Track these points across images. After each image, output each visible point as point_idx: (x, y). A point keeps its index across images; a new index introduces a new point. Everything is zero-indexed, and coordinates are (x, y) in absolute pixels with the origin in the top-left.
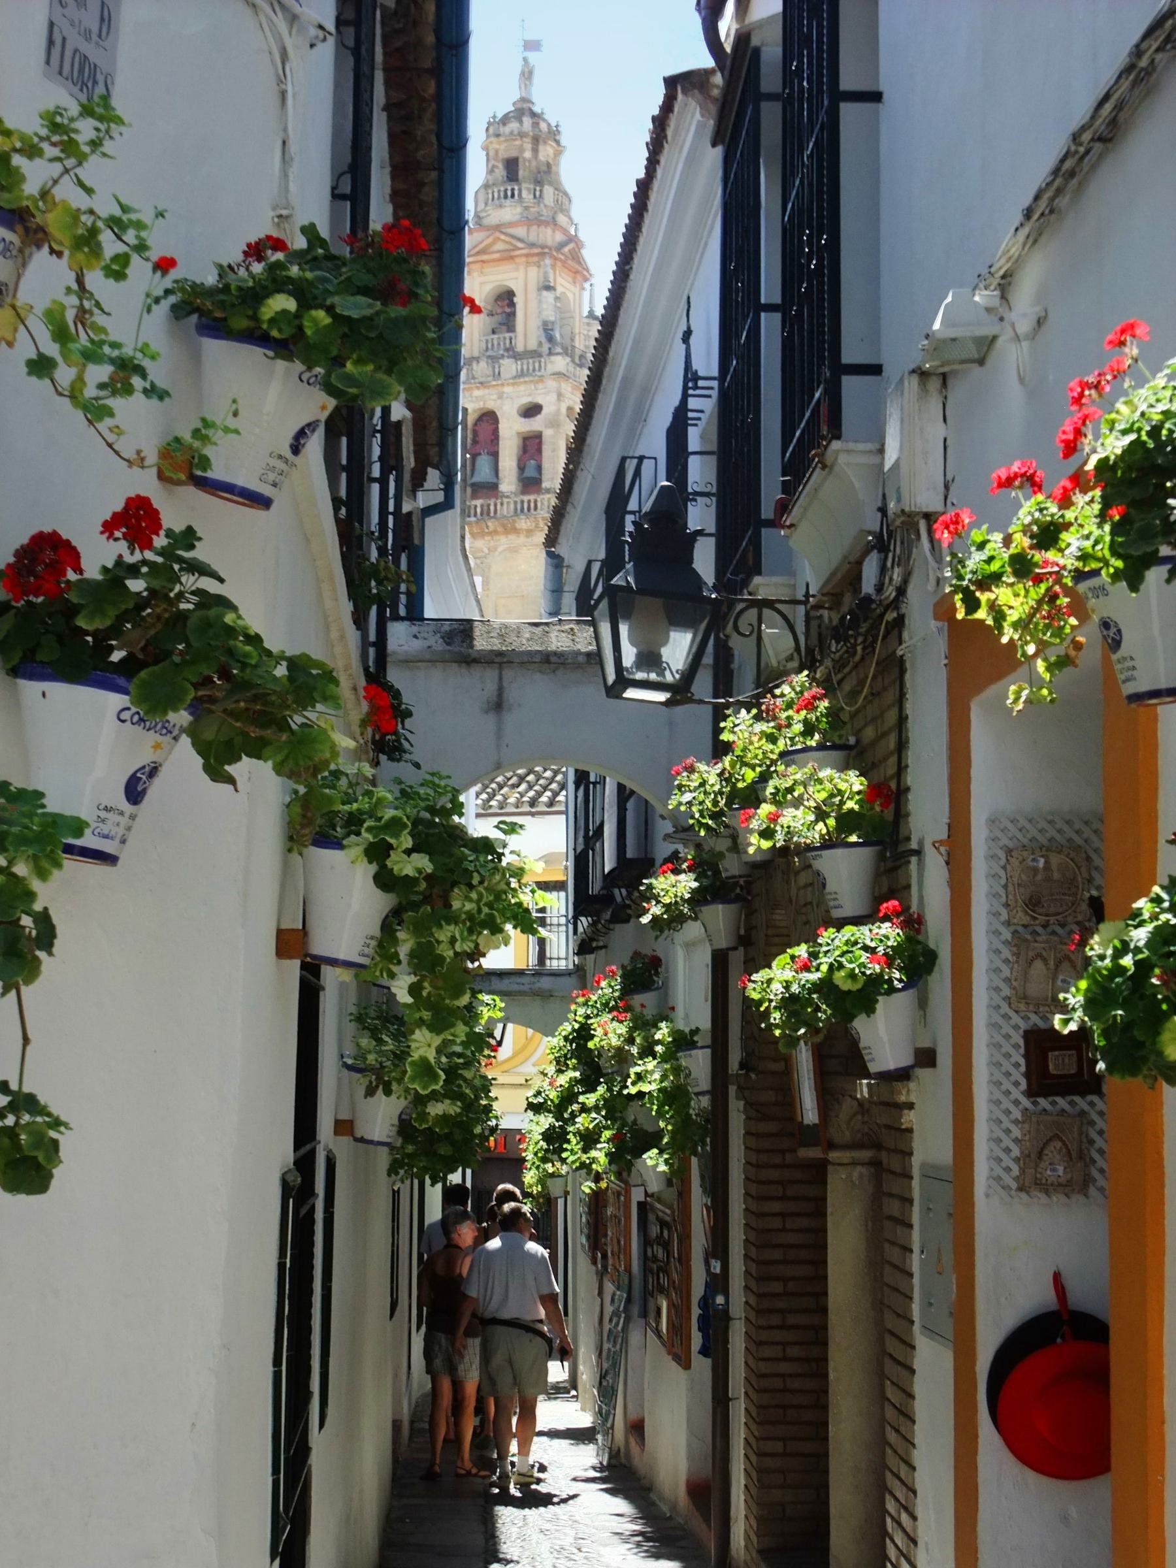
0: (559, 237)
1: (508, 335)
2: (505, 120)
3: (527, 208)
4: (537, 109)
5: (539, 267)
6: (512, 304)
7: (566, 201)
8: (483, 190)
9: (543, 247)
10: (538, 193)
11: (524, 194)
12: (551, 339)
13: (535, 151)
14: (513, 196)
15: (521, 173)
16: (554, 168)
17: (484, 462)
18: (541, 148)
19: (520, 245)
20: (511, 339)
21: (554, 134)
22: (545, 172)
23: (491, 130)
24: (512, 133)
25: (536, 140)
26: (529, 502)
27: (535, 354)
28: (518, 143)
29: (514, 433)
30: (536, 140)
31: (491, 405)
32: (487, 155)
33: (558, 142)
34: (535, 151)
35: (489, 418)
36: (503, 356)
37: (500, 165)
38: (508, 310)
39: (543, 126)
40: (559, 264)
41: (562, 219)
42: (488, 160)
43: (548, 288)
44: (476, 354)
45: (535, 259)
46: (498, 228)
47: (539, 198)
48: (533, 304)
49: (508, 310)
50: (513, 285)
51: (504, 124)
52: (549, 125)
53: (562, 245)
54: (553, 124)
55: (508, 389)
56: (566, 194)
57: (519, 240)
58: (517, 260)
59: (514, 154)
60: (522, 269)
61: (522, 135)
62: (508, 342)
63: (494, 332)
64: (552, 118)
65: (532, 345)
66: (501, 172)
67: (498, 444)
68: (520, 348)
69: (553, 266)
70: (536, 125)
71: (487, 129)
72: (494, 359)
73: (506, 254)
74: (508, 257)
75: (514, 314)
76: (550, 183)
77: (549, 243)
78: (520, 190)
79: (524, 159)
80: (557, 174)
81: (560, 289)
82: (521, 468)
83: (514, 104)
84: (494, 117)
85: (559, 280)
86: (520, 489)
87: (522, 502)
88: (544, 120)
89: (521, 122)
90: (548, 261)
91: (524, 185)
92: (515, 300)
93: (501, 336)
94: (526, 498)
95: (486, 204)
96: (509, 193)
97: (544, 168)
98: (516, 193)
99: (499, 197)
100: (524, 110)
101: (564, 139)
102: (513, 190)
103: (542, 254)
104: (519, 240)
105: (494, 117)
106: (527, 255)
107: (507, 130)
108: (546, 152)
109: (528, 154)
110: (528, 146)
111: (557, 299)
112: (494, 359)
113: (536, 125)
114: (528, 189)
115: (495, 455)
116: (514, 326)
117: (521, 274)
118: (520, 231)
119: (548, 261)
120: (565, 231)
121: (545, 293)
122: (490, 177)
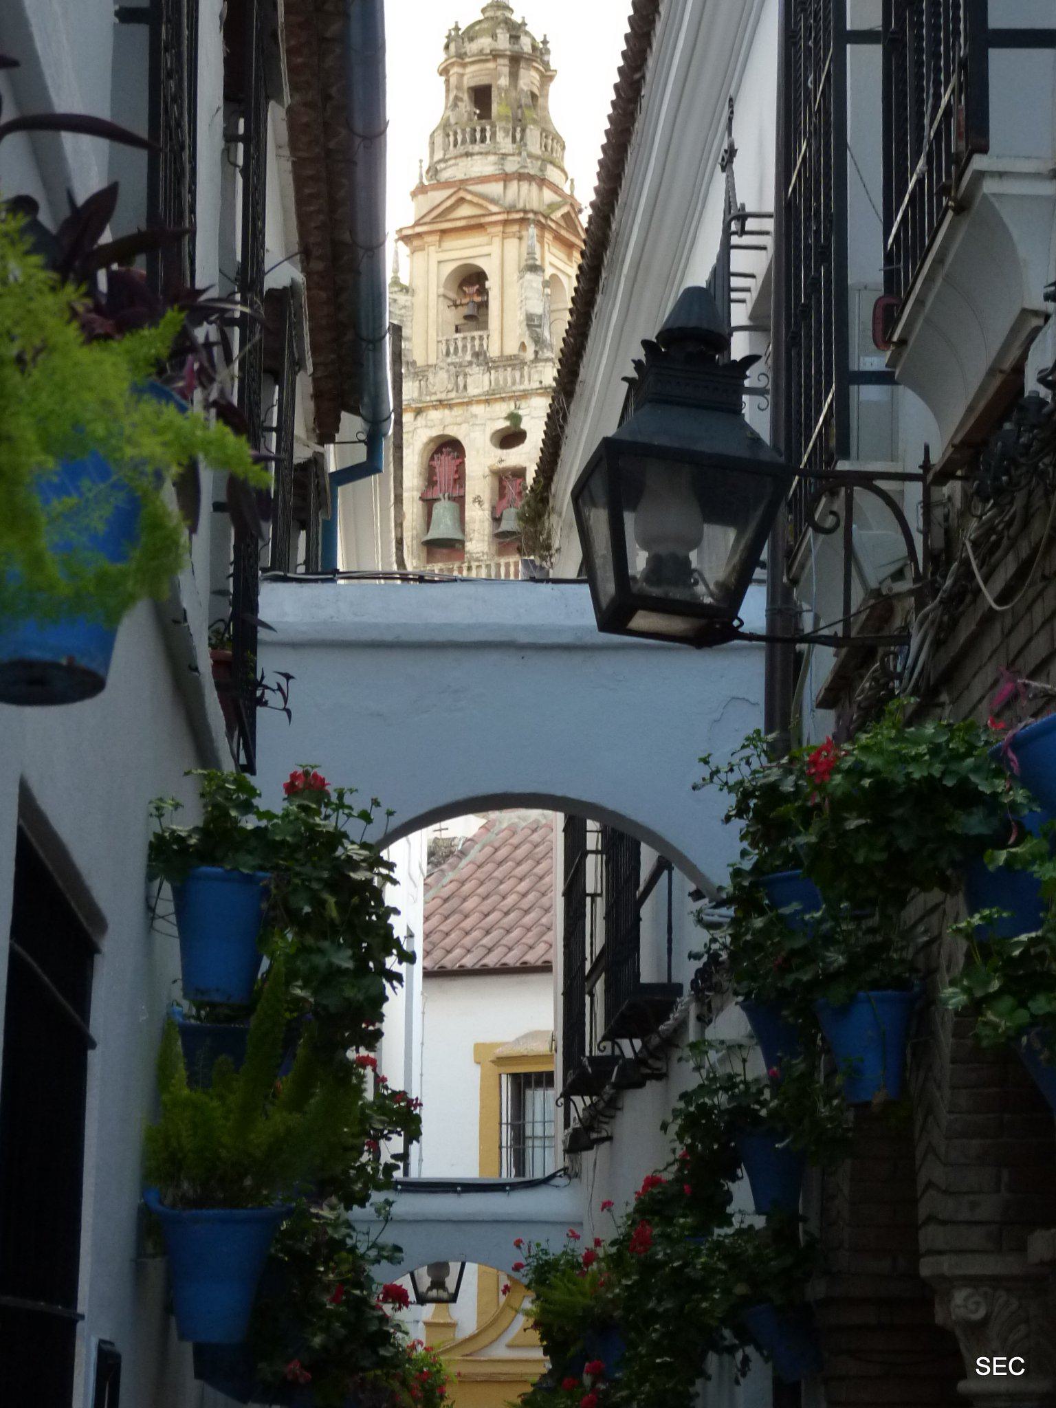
0: (549, 196)
1: (476, 334)
2: (471, 34)
3: (505, 155)
4: (516, 18)
5: (520, 238)
6: (483, 291)
7: (557, 147)
8: (440, 132)
9: (525, 212)
10: (518, 136)
11: (500, 135)
12: (538, 341)
13: (514, 76)
14: (483, 140)
15: (495, 108)
16: (540, 101)
17: (443, 510)
18: (522, 72)
19: (494, 209)
20: (481, 338)
21: (539, 53)
22: (528, 107)
23: (452, 47)
24: (481, 52)
25: (516, 60)
26: (507, 565)
27: (514, 362)
28: (491, 65)
29: (487, 472)
30: (516, 60)
31: (452, 432)
32: (447, 81)
33: (546, 65)
34: (514, 76)
35: (449, 447)
36: (470, 363)
37: (466, 97)
38: (478, 299)
39: (525, 45)
40: (548, 236)
41: (552, 174)
42: (448, 91)
43: (534, 268)
44: (432, 361)
45: (515, 228)
46: (462, 184)
47: (520, 142)
48: (513, 291)
49: (478, 299)
50: (482, 263)
51: (471, 39)
52: (533, 39)
53: (553, 207)
54: (539, 39)
55: (478, 409)
56: (557, 138)
57: (493, 201)
58: (491, 230)
59: (483, 81)
60: (497, 241)
61: (495, 55)
62: (477, 342)
63: (457, 331)
64: (536, 29)
65: (512, 348)
66: (466, 106)
67: (463, 486)
68: (494, 352)
69: (541, 239)
70: (515, 38)
71: (447, 47)
72: (460, 370)
73: (473, 222)
74: (475, 227)
75: (484, 305)
76: (535, 122)
77: (535, 206)
78: (494, 134)
79: (499, 88)
80: (545, 108)
81: (549, 271)
82: (497, 520)
83: (484, 11)
84: (457, 29)
85: (549, 258)
86: (494, 548)
87: (498, 566)
88: (527, 33)
89: (494, 36)
90: (533, 230)
91: (499, 125)
92: (487, 284)
93: (469, 335)
94: (503, 561)
95: (446, 150)
96: (478, 136)
97: (526, 100)
98: (488, 135)
99: (464, 142)
100: (499, 18)
101: (554, 61)
102: (483, 130)
103: (523, 221)
104: (493, 201)
105: (457, 29)
106: (506, 223)
107: (472, 47)
108: (529, 78)
109: (504, 81)
110: (506, 70)
111: (546, 284)
112: (460, 370)
113: (515, 38)
114: (506, 131)
115: (460, 501)
116: (486, 322)
117: (495, 249)
118: (495, 189)
119: (533, 230)
120: (556, 189)
121: (529, 276)
122: (449, 113)
